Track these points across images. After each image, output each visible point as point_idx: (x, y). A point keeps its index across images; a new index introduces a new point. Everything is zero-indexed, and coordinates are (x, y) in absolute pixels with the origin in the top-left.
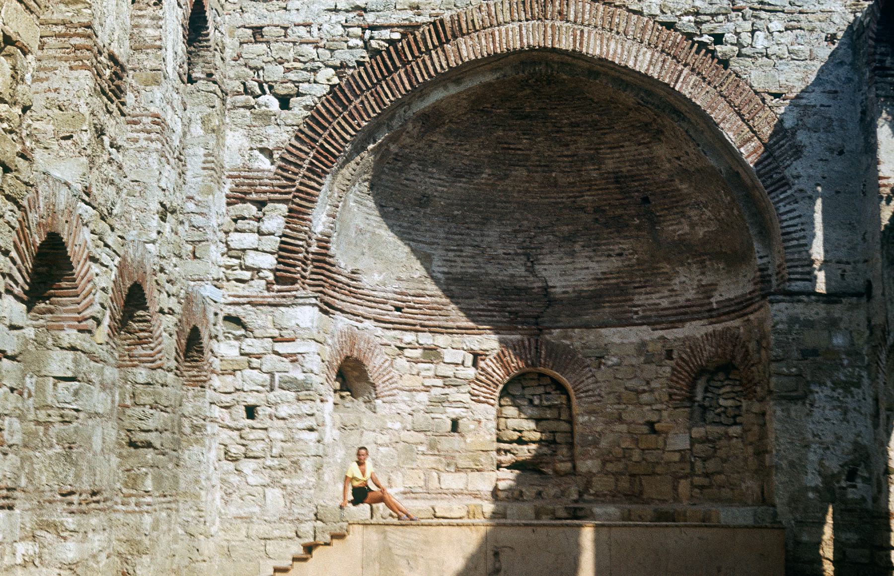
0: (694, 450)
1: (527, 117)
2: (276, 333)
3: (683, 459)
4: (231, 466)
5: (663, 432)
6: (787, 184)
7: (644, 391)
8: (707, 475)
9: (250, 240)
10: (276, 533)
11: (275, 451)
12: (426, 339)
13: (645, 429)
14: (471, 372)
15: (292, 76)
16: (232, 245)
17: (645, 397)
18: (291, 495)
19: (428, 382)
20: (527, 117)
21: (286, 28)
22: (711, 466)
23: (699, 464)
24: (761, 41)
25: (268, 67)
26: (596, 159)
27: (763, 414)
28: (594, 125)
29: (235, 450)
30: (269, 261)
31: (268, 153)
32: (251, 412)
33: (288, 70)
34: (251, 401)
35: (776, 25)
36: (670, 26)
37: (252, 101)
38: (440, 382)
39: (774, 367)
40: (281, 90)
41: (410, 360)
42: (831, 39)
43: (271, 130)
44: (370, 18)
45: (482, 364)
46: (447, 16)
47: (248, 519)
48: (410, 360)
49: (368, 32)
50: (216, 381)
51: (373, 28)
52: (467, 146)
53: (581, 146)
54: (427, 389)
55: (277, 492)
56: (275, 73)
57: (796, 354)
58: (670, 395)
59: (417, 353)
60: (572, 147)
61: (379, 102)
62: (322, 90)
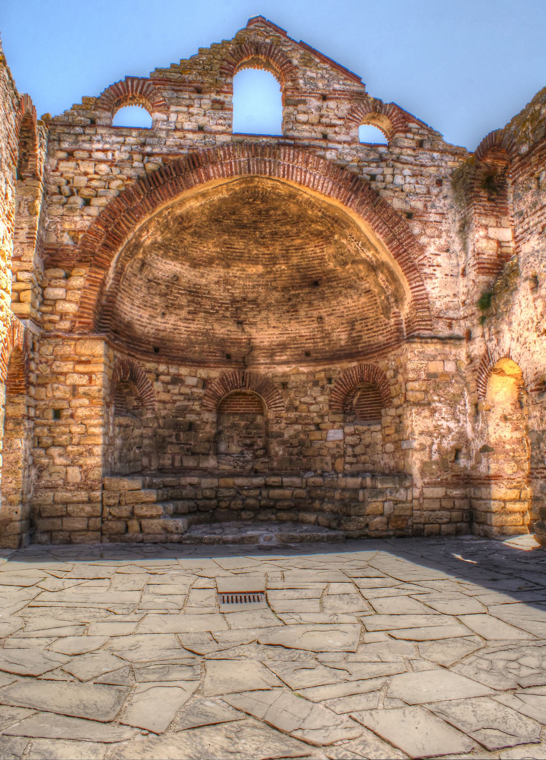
0: (346, 440)
1: (244, 227)
2: (77, 358)
3: (338, 446)
4: (42, 452)
5: (326, 430)
6: (416, 269)
7: (312, 404)
8: (355, 456)
9: (59, 292)
10: (75, 499)
11: (75, 440)
13: (313, 428)
16: (47, 297)
17: (312, 408)
18: (85, 472)
19: (175, 398)
20: (244, 227)
21: (90, 152)
23: (349, 450)
24: (399, 180)
25: (76, 178)
26: (286, 257)
27: (400, 416)
28: (287, 235)
32: (57, 414)
33: (91, 180)
34: (59, 405)
35: (407, 172)
36: (343, 168)
37: (64, 200)
38: (182, 398)
39: (410, 385)
40: (86, 192)
41: (163, 382)
44: (148, 149)
45: (210, 387)
48: (163, 382)
49: (146, 158)
51: (150, 155)
52: (205, 245)
53: (277, 249)
54: (174, 402)
55: (76, 470)
56: (82, 181)
57: (423, 377)
58: (330, 406)
59: (167, 378)
60: (271, 249)
62: (112, 193)
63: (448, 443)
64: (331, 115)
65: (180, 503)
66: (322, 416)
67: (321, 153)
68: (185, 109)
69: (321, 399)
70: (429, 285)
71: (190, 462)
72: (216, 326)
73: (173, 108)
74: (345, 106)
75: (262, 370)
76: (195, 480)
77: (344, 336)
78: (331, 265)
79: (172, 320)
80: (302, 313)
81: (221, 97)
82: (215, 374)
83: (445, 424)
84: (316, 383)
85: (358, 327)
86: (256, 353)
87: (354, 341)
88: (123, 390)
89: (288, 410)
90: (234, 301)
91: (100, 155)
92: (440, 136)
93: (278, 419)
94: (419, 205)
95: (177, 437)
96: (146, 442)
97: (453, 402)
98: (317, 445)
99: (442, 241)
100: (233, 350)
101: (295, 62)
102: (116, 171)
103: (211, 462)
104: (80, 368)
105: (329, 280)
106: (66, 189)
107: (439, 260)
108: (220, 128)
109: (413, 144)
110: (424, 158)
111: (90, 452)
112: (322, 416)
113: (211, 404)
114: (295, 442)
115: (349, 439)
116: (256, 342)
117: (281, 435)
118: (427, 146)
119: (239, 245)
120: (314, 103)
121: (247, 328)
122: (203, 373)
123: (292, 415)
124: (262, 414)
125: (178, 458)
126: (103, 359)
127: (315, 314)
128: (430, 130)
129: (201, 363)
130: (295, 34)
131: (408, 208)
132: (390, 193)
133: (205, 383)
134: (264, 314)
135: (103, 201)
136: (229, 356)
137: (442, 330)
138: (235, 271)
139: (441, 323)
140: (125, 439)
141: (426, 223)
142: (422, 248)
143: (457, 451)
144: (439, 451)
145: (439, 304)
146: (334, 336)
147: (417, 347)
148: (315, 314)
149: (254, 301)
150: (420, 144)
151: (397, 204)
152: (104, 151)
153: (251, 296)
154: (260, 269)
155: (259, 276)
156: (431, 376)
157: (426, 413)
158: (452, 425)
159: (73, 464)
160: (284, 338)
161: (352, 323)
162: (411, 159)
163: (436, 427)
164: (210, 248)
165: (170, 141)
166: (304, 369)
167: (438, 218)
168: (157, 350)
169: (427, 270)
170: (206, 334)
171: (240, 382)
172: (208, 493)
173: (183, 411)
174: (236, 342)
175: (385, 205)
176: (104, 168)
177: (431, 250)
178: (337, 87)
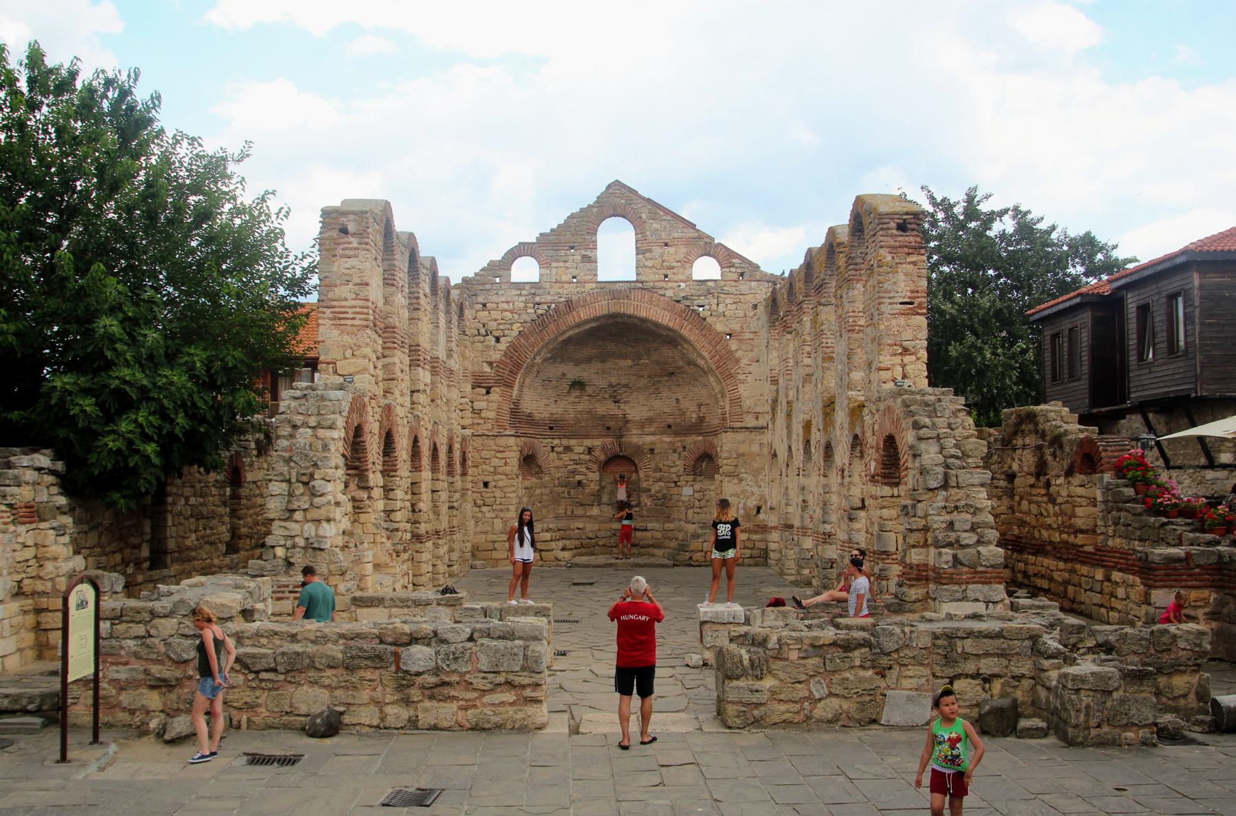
12: (565, 442)
14: (587, 457)
15: (501, 327)
17: (673, 470)
18: (505, 522)
22: (703, 503)
24: (721, 308)
29: (480, 502)
30: (492, 415)
31: (490, 364)
42: (755, 307)
43: (492, 353)
44: (537, 299)
46: (574, 298)
47: (485, 533)
50: (470, 471)
61: (542, 339)
62: (515, 333)
63: (752, 503)
64: (671, 259)
65: (567, 542)
66: (679, 476)
67: (661, 292)
68: (562, 264)
69: (678, 463)
70: (742, 390)
71: (579, 511)
72: (597, 405)
73: (554, 264)
74: (683, 250)
75: (635, 440)
76: (581, 525)
77: (694, 416)
78: (681, 364)
79: (562, 404)
80: (664, 395)
81: (588, 253)
82: (597, 443)
83: (749, 489)
84: (675, 451)
85: (703, 409)
86: (629, 426)
87: (701, 419)
88: (529, 461)
89: (655, 471)
90: (611, 385)
91: (505, 306)
92: (758, 267)
93: (647, 477)
94: (737, 327)
95: (569, 493)
96: (545, 497)
97: (756, 473)
98: (675, 497)
99: (753, 354)
100: (612, 424)
101: (644, 216)
102: (516, 316)
103: (595, 511)
104: (499, 455)
105: (681, 373)
106: (483, 331)
107: (750, 369)
108: (588, 278)
109: (735, 276)
110: (744, 287)
111: (508, 510)
112: (679, 476)
113: (595, 467)
114: (660, 495)
115: (697, 495)
116: (630, 417)
117: (649, 490)
118: (746, 277)
119: (611, 347)
120: (657, 251)
121: (622, 406)
122: (588, 443)
123: (658, 475)
124: (637, 471)
125: (569, 508)
126: (515, 448)
127: (674, 396)
128: (750, 263)
129: (587, 437)
130: (643, 192)
131: (728, 331)
132: (715, 319)
133: (590, 450)
134: (635, 394)
135: (509, 339)
136: (608, 428)
137: (750, 422)
138: (609, 364)
139: (750, 416)
140: (530, 497)
141: (741, 340)
142: (738, 361)
143: (759, 509)
144: (744, 508)
145: (747, 403)
146: (688, 414)
147: (730, 435)
148: (674, 396)
149: (626, 386)
150: (742, 275)
151: (719, 327)
152: (508, 302)
153: (624, 382)
154: (629, 362)
155: (631, 367)
156: (740, 455)
157: (736, 481)
158: (755, 490)
159: (497, 517)
160: (651, 414)
161: (699, 406)
162: (733, 290)
163: (743, 492)
164: (588, 351)
165: (553, 291)
166: (667, 439)
167: (751, 336)
168: (551, 428)
169: (741, 377)
170: (590, 412)
171: (617, 448)
172: (590, 535)
173: (574, 472)
174: (613, 417)
175: (710, 328)
176: (508, 314)
177: (745, 361)
178: (676, 235)
